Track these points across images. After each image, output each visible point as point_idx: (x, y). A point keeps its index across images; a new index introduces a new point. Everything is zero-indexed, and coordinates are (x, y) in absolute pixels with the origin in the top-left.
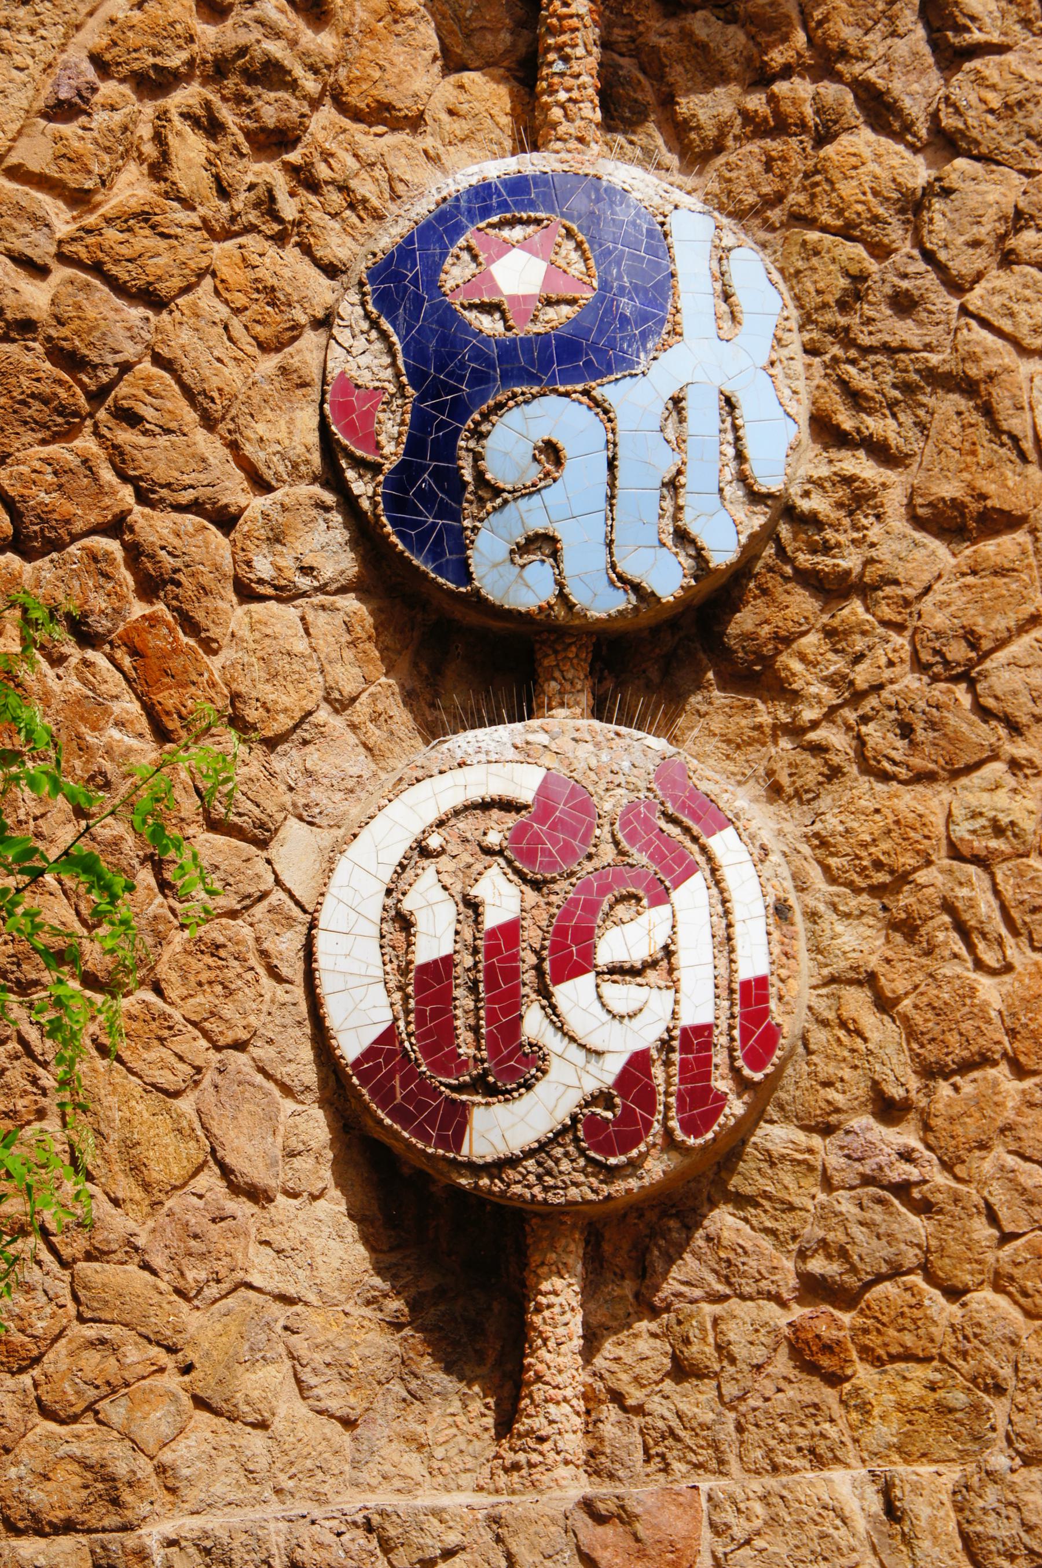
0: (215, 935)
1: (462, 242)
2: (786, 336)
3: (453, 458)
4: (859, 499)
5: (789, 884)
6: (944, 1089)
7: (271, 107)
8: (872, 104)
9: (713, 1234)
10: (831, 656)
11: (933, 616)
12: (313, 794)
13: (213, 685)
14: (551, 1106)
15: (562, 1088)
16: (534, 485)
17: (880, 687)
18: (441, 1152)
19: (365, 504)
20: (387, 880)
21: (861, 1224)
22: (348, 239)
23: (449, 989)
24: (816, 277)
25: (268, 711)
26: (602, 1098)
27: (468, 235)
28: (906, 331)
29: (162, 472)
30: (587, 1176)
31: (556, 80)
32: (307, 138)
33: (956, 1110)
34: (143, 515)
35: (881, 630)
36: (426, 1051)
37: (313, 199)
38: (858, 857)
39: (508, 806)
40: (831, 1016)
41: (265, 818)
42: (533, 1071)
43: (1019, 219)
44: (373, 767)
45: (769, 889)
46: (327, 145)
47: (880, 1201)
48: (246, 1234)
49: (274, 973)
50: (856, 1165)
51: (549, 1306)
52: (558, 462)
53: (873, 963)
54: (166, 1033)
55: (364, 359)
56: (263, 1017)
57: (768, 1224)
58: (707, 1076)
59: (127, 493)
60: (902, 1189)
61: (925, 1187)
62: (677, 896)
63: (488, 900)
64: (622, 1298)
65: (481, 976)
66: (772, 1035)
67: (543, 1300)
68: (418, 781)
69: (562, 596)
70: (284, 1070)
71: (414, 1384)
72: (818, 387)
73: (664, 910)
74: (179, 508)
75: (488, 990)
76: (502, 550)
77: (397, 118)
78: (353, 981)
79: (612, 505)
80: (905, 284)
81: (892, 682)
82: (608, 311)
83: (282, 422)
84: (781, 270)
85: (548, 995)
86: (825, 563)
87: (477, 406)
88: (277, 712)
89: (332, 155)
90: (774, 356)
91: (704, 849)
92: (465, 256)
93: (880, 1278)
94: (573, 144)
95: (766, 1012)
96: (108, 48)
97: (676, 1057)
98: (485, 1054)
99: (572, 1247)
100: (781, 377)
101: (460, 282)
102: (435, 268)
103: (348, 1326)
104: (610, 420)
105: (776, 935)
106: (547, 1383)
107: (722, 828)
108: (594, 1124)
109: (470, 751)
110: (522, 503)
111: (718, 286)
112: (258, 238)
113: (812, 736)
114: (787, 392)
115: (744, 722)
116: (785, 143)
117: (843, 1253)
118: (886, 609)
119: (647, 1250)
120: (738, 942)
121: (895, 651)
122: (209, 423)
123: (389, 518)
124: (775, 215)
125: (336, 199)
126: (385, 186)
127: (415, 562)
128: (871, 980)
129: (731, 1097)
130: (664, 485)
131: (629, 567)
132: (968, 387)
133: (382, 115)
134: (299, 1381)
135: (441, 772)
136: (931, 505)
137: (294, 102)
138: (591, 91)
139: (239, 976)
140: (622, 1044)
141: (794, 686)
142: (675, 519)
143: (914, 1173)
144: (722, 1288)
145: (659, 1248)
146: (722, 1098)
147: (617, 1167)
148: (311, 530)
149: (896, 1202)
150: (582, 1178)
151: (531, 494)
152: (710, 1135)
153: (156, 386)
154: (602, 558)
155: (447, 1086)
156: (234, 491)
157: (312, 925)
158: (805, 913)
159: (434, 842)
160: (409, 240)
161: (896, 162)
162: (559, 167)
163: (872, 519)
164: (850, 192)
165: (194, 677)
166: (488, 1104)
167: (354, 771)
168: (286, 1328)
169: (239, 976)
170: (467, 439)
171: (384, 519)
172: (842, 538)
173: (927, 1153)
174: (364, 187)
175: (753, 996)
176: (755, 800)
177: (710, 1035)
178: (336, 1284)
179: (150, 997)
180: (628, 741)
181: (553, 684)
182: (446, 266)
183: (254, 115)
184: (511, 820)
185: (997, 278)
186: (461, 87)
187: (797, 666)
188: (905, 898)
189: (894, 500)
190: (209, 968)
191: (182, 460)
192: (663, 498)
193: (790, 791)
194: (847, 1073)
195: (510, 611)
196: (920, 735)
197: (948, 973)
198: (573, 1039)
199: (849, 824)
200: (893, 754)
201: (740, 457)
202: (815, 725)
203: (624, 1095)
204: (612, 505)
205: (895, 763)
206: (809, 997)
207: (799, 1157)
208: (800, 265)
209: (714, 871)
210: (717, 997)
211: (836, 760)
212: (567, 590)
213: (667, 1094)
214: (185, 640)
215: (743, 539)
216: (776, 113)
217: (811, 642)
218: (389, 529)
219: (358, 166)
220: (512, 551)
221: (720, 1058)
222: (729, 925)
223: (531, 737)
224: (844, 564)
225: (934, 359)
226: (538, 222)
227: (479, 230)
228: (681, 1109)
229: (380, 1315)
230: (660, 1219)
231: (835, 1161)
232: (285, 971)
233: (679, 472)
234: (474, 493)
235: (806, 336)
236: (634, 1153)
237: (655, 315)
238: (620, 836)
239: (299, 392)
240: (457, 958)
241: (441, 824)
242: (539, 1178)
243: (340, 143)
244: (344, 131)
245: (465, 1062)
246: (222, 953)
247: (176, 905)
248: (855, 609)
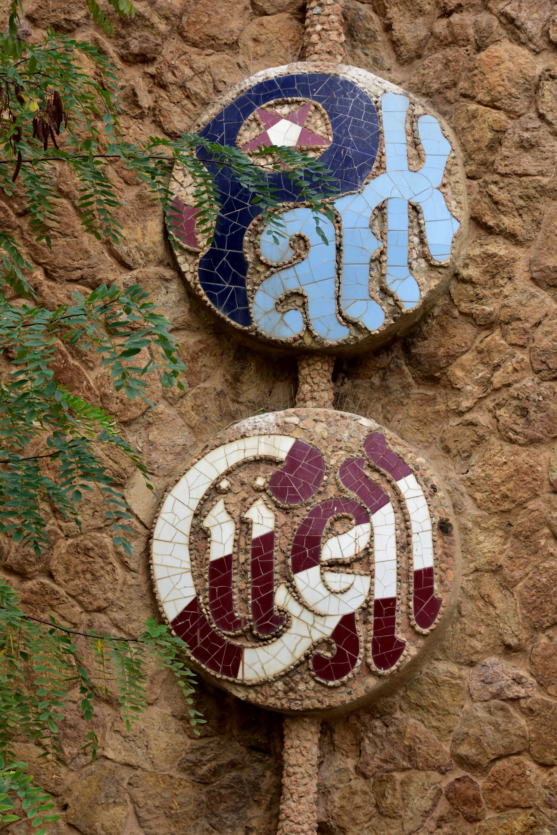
0: (86, 542)
1: (251, 117)
2: (454, 168)
3: (240, 247)
4: (496, 268)
5: (450, 510)
6: (543, 640)
8: (510, 26)
9: (402, 730)
10: (481, 367)
11: (541, 340)
12: (153, 455)
13: (89, 389)
14: (292, 649)
15: (299, 638)
16: (290, 263)
17: (509, 385)
18: (225, 677)
19: (189, 277)
20: (194, 509)
21: (490, 724)
22: (186, 118)
23: (229, 576)
24: (474, 132)
25: (124, 404)
26: (325, 642)
27: (255, 111)
28: (527, 162)
29: (61, 260)
30: (315, 692)
31: (315, 18)
32: (160, 59)
33: (550, 651)
34: (49, 287)
35: (510, 350)
36: (216, 614)
37: (163, 94)
38: (493, 493)
39: (270, 461)
40: (475, 593)
41: (121, 471)
42: (281, 627)
44: (194, 439)
45: (436, 513)
46: (173, 62)
47: (502, 709)
48: (104, 726)
49: (125, 565)
50: (488, 686)
51: (294, 773)
52: (306, 248)
53: (502, 560)
54: (55, 602)
55: (186, 187)
56: (118, 594)
57: (434, 724)
58: (392, 630)
59: (39, 274)
60: (515, 700)
61: (529, 700)
62: (376, 518)
63: (255, 520)
64: (346, 770)
65: (249, 568)
66: (436, 604)
67: (291, 770)
68: (217, 447)
69: (308, 330)
70: (131, 626)
71: (214, 820)
72: (475, 199)
73: (365, 527)
74: (71, 281)
75: (253, 576)
76: (270, 303)
77: (219, 45)
78: (173, 571)
79: (339, 274)
80: (526, 135)
81: (516, 382)
82: (338, 154)
83: (139, 228)
84: (454, 129)
85: (290, 580)
86: (476, 308)
87: (255, 216)
88: (130, 405)
89: (176, 68)
90: (445, 181)
91: (394, 488)
92: (254, 125)
93: (500, 757)
94: (325, 56)
95: (431, 590)
96: (36, 11)
97: (372, 618)
98: (251, 616)
99: (310, 736)
100: (450, 193)
101: (248, 140)
103: (171, 784)
104: (338, 222)
105: (440, 542)
106: (292, 821)
107: (406, 475)
108: (319, 661)
109: (250, 428)
110: (284, 274)
111: (410, 139)
112: (126, 118)
113: (468, 417)
114: (454, 203)
115: (428, 409)
116: (458, 51)
117: (478, 741)
118: (513, 337)
119: (362, 739)
120: (415, 546)
121: (517, 362)
122: (91, 229)
123: (203, 285)
124: (450, 94)
125: (178, 94)
126: (211, 86)
127: (218, 312)
128: (497, 570)
129: (407, 644)
130: (372, 261)
131: (352, 313)
134: (138, 817)
135: (231, 441)
136: (541, 270)
137: (152, 38)
138: (337, 24)
139: (102, 568)
140: (337, 609)
141: (458, 386)
142: (381, 282)
143: (522, 692)
144: (405, 764)
145: (369, 738)
146: (402, 645)
147: (334, 687)
148: (158, 294)
149: (511, 709)
150: (313, 694)
151: (288, 268)
152: (394, 668)
153: (58, 209)
154: (332, 308)
155: (229, 636)
156: (108, 271)
157: (150, 537)
158: (460, 529)
159: (224, 484)
160: (219, 116)
161: (522, 61)
162: (313, 70)
163: (506, 280)
164: (495, 79)
165: (77, 385)
166: (253, 647)
167: (181, 441)
168: (129, 784)
169: (102, 568)
170: (250, 235)
171: (199, 286)
172: (487, 292)
173: (531, 679)
174: (196, 87)
175: (423, 580)
176: (433, 458)
177: (394, 604)
178: (163, 758)
179: (46, 581)
180: (349, 421)
181: (306, 386)
182: (241, 131)
183: (126, 46)
184: (272, 470)
186: (262, 25)
187: (460, 373)
188: (521, 520)
189: (520, 270)
190: (83, 562)
191: (73, 253)
192: (371, 269)
193: (454, 452)
194: (483, 629)
195: (276, 341)
196: (532, 415)
197: (547, 565)
198: (306, 607)
199: (488, 472)
200: (515, 427)
201: (422, 242)
202: (470, 409)
203: (338, 642)
204: (339, 274)
205: (516, 433)
206: (462, 581)
207: (454, 682)
208: (465, 125)
209: (400, 501)
210: (399, 581)
211: (481, 432)
212: (311, 328)
213: (366, 641)
214: (71, 361)
215: (424, 294)
216: (452, 34)
217: (467, 358)
218: (202, 292)
219: (193, 73)
220: (277, 303)
221: (399, 618)
222: (409, 536)
223: (288, 419)
224: (488, 309)
225: (545, 181)
226: (298, 102)
227: (262, 109)
228: (375, 651)
229: (192, 778)
230: (370, 720)
231: (475, 684)
232: (133, 565)
233: (382, 253)
234: (254, 268)
235: (468, 168)
236: (345, 678)
237: (369, 157)
238: (339, 480)
239: (150, 210)
240: (235, 557)
241: (228, 473)
242: (286, 693)
243: (182, 60)
244: (185, 53)
245: (239, 622)
246: (91, 554)
247: (63, 524)
248: (496, 336)
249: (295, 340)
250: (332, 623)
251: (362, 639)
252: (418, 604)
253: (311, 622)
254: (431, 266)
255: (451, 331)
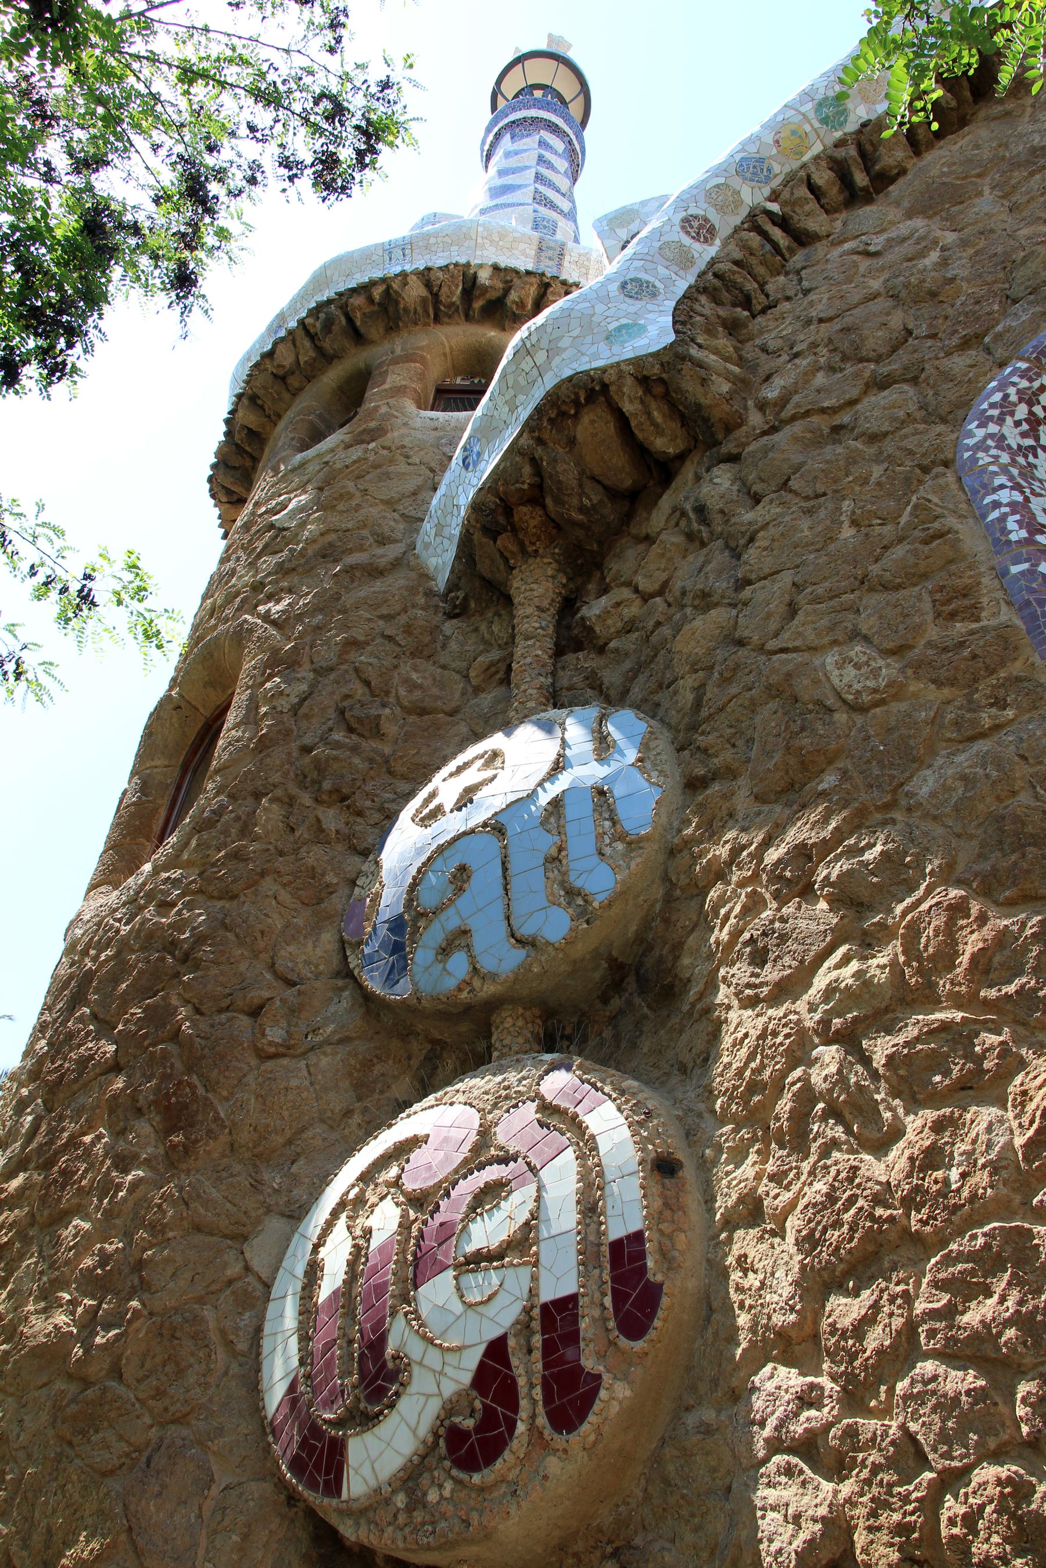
14: (413, 1424)
97: (537, 1340)
105: (656, 1189)
108: (455, 1437)
110: (443, 916)
129: (606, 1378)
152: (585, 1428)
177: (576, 1306)
203: (483, 1394)
228: (548, 1399)
233: (560, 849)
249: (460, 989)
250: (472, 1359)
251: (521, 1381)
252: (619, 1298)
253: (439, 1368)
254: (630, 843)
255: (674, 918)
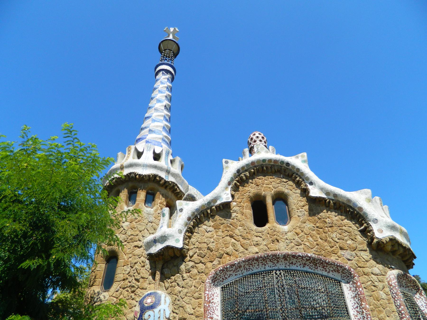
7: (133, 289)
28: (178, 303)
43: (187, 293)
102: (143, 301)
125: (138, 296)
132: (183, 307)
133: (142, 289)
174: (140, 295)
185: (186, 298)
